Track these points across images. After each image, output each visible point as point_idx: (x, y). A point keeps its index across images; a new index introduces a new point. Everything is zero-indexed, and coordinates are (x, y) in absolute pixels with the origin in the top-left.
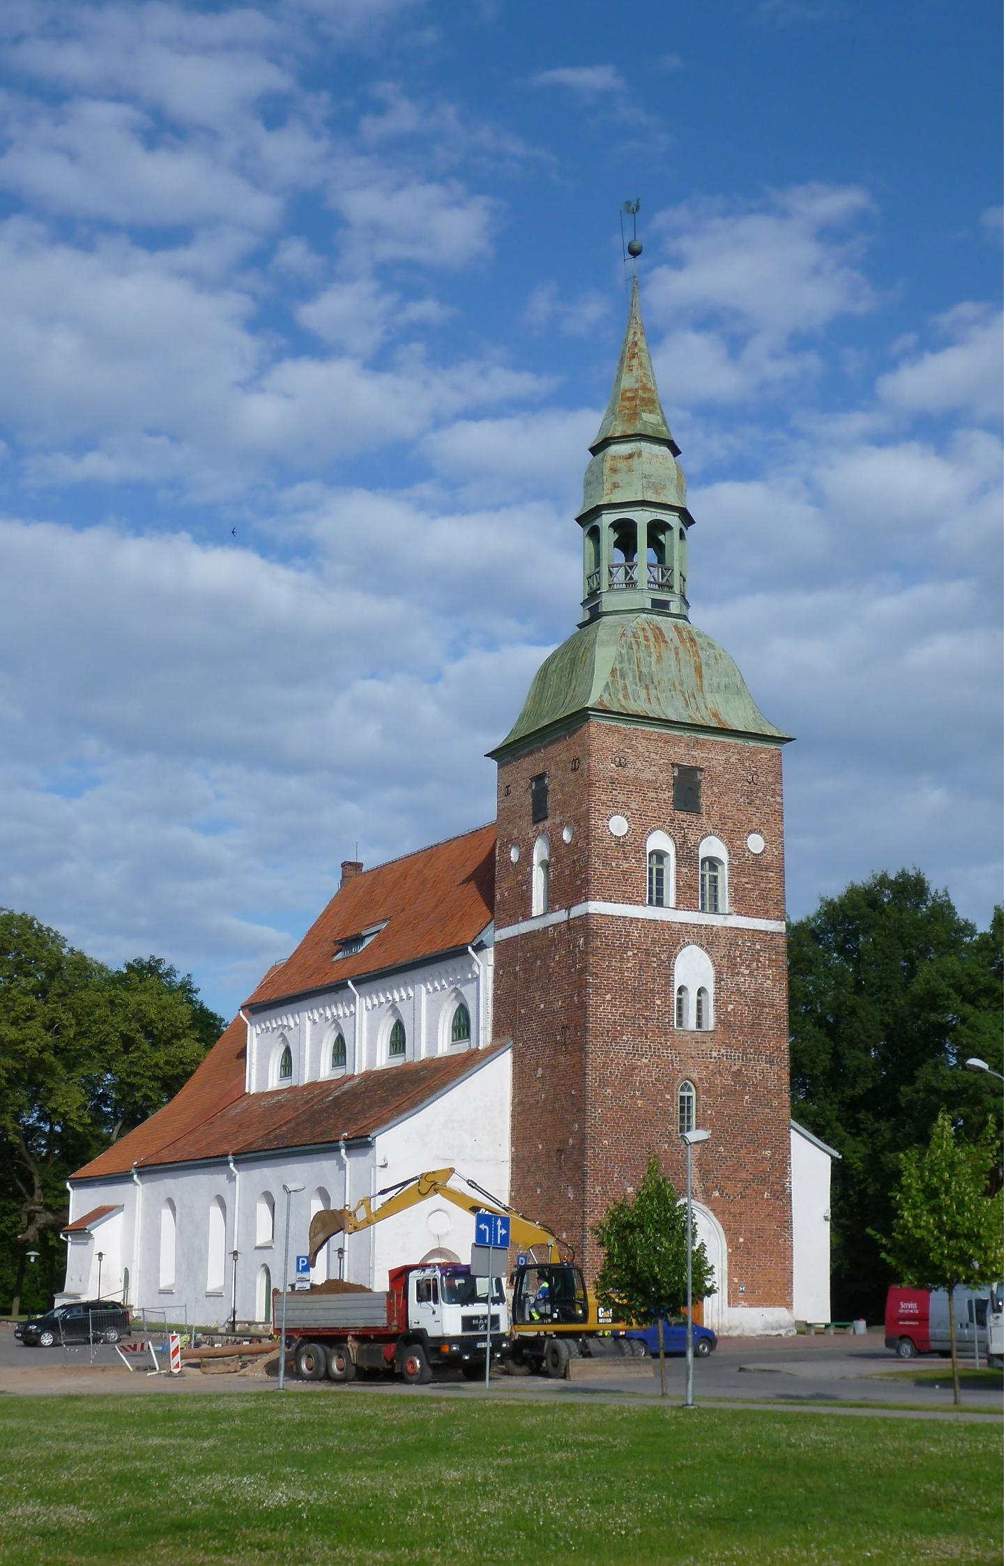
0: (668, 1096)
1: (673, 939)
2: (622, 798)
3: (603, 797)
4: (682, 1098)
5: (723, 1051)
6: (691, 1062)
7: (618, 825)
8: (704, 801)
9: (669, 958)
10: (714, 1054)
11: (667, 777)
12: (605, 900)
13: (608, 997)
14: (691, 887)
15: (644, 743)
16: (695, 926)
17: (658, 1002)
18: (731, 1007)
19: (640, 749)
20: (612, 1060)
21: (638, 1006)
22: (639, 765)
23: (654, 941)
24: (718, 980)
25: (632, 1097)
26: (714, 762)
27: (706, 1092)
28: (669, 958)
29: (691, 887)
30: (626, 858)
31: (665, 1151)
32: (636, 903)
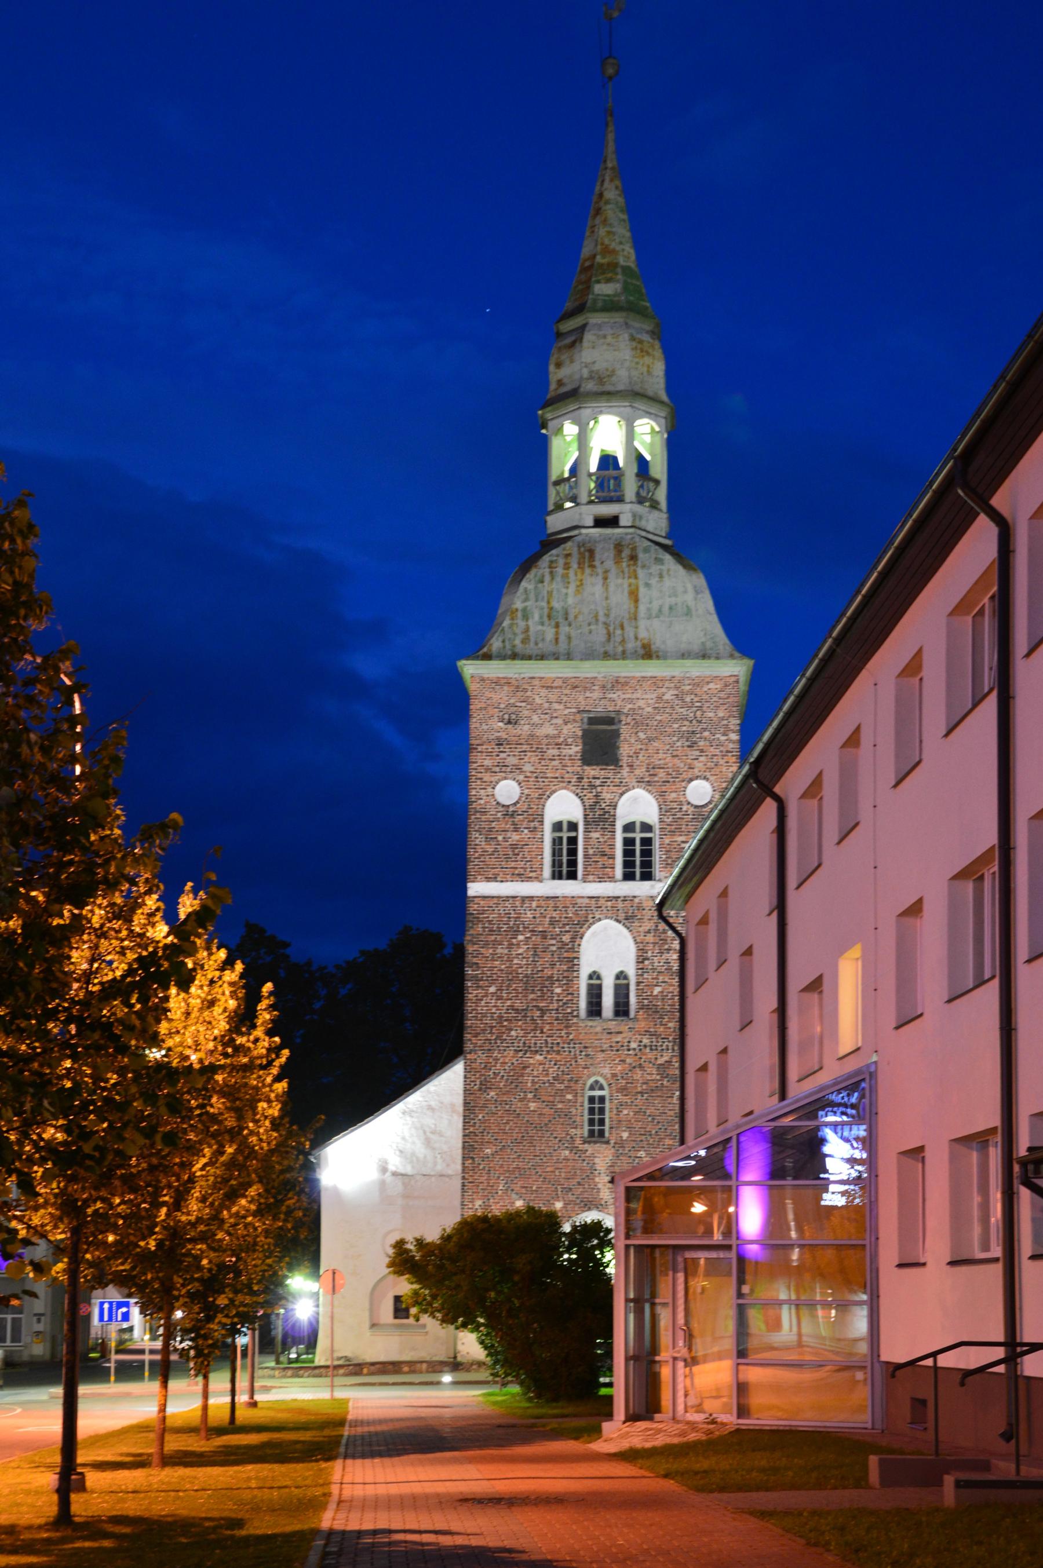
0: (569, 1097)
1: (578, 918)
2: (512, 761)
3: (487, 762)
4: (592, 1100)
5: (646, 1041)
6: (601, 1056)
7: (507, 791)
8: (625, 751)
9: (573, 939)
10: (633, 1045)
11: (574, 730)
12: (488, 879)
13: (492, 989)
14: (604, 854)
15: (544, 692)
16: (609, 899)
17: (558, 990)
18: (657, 990)
19: (538, 701)
20: (496, 1060)
21: (532, 996)
22: (535, 719)
23: (553, 922)
24: (641, 959)
25: (521, 1100)
26: (641, 703)
27: (623, 1090)
28: (573, 939)
29: (604, 854)
30: (516, 830)
31: (566, 1159)
32: (529, 879)
